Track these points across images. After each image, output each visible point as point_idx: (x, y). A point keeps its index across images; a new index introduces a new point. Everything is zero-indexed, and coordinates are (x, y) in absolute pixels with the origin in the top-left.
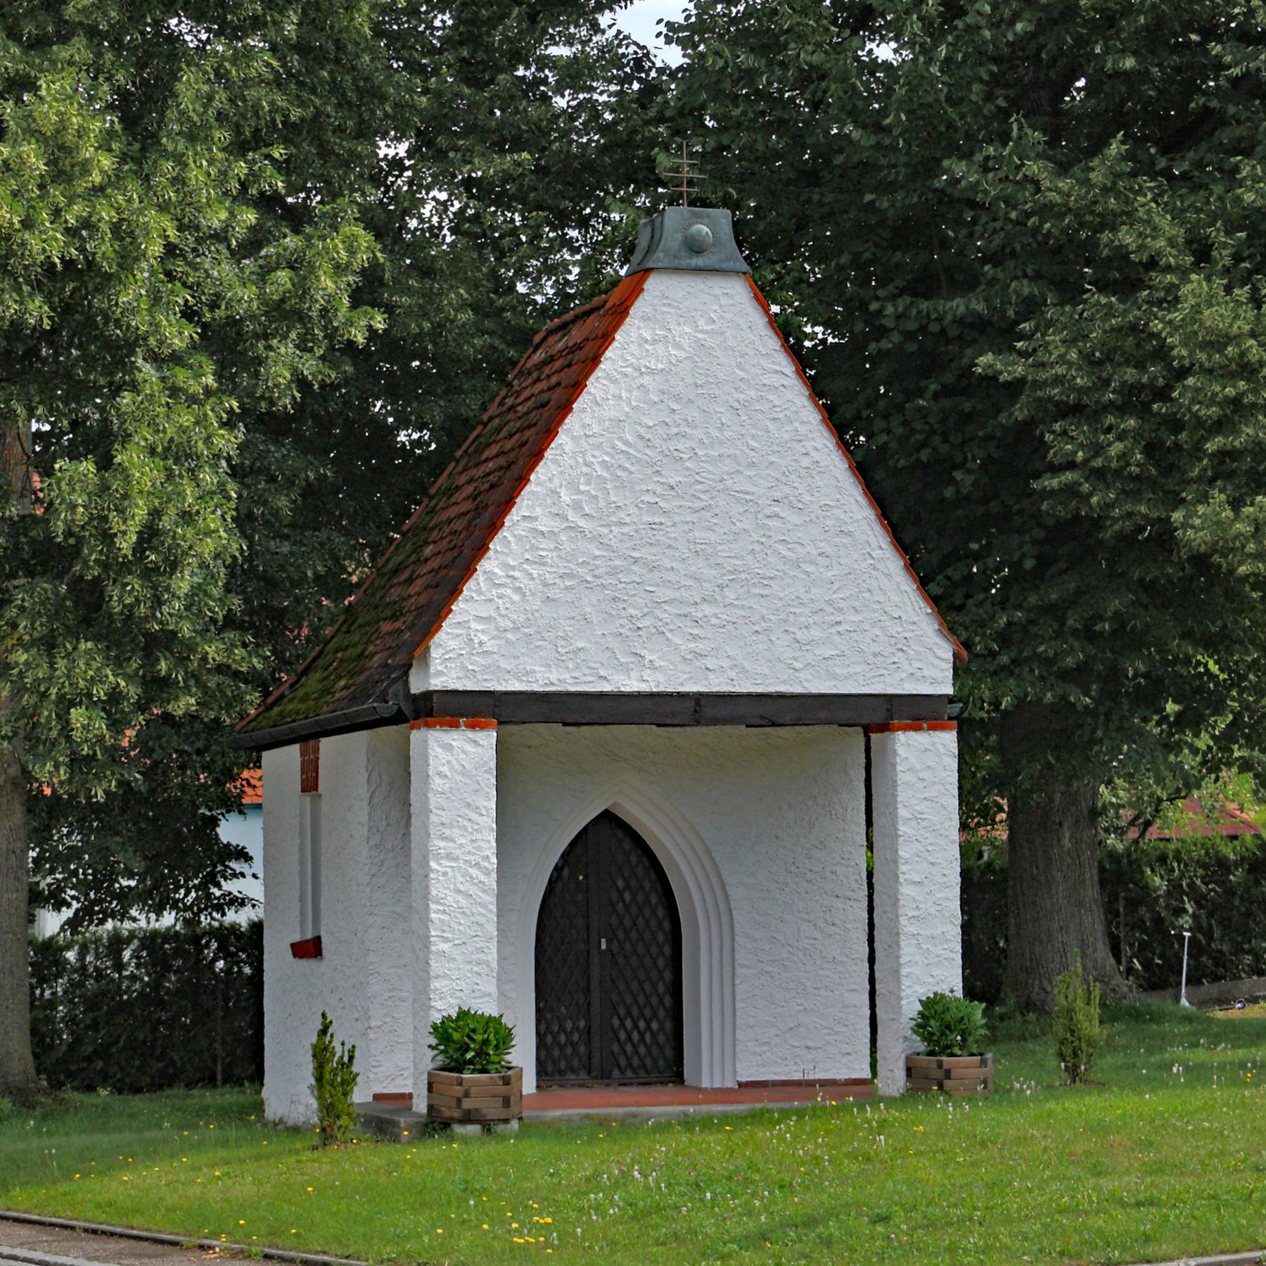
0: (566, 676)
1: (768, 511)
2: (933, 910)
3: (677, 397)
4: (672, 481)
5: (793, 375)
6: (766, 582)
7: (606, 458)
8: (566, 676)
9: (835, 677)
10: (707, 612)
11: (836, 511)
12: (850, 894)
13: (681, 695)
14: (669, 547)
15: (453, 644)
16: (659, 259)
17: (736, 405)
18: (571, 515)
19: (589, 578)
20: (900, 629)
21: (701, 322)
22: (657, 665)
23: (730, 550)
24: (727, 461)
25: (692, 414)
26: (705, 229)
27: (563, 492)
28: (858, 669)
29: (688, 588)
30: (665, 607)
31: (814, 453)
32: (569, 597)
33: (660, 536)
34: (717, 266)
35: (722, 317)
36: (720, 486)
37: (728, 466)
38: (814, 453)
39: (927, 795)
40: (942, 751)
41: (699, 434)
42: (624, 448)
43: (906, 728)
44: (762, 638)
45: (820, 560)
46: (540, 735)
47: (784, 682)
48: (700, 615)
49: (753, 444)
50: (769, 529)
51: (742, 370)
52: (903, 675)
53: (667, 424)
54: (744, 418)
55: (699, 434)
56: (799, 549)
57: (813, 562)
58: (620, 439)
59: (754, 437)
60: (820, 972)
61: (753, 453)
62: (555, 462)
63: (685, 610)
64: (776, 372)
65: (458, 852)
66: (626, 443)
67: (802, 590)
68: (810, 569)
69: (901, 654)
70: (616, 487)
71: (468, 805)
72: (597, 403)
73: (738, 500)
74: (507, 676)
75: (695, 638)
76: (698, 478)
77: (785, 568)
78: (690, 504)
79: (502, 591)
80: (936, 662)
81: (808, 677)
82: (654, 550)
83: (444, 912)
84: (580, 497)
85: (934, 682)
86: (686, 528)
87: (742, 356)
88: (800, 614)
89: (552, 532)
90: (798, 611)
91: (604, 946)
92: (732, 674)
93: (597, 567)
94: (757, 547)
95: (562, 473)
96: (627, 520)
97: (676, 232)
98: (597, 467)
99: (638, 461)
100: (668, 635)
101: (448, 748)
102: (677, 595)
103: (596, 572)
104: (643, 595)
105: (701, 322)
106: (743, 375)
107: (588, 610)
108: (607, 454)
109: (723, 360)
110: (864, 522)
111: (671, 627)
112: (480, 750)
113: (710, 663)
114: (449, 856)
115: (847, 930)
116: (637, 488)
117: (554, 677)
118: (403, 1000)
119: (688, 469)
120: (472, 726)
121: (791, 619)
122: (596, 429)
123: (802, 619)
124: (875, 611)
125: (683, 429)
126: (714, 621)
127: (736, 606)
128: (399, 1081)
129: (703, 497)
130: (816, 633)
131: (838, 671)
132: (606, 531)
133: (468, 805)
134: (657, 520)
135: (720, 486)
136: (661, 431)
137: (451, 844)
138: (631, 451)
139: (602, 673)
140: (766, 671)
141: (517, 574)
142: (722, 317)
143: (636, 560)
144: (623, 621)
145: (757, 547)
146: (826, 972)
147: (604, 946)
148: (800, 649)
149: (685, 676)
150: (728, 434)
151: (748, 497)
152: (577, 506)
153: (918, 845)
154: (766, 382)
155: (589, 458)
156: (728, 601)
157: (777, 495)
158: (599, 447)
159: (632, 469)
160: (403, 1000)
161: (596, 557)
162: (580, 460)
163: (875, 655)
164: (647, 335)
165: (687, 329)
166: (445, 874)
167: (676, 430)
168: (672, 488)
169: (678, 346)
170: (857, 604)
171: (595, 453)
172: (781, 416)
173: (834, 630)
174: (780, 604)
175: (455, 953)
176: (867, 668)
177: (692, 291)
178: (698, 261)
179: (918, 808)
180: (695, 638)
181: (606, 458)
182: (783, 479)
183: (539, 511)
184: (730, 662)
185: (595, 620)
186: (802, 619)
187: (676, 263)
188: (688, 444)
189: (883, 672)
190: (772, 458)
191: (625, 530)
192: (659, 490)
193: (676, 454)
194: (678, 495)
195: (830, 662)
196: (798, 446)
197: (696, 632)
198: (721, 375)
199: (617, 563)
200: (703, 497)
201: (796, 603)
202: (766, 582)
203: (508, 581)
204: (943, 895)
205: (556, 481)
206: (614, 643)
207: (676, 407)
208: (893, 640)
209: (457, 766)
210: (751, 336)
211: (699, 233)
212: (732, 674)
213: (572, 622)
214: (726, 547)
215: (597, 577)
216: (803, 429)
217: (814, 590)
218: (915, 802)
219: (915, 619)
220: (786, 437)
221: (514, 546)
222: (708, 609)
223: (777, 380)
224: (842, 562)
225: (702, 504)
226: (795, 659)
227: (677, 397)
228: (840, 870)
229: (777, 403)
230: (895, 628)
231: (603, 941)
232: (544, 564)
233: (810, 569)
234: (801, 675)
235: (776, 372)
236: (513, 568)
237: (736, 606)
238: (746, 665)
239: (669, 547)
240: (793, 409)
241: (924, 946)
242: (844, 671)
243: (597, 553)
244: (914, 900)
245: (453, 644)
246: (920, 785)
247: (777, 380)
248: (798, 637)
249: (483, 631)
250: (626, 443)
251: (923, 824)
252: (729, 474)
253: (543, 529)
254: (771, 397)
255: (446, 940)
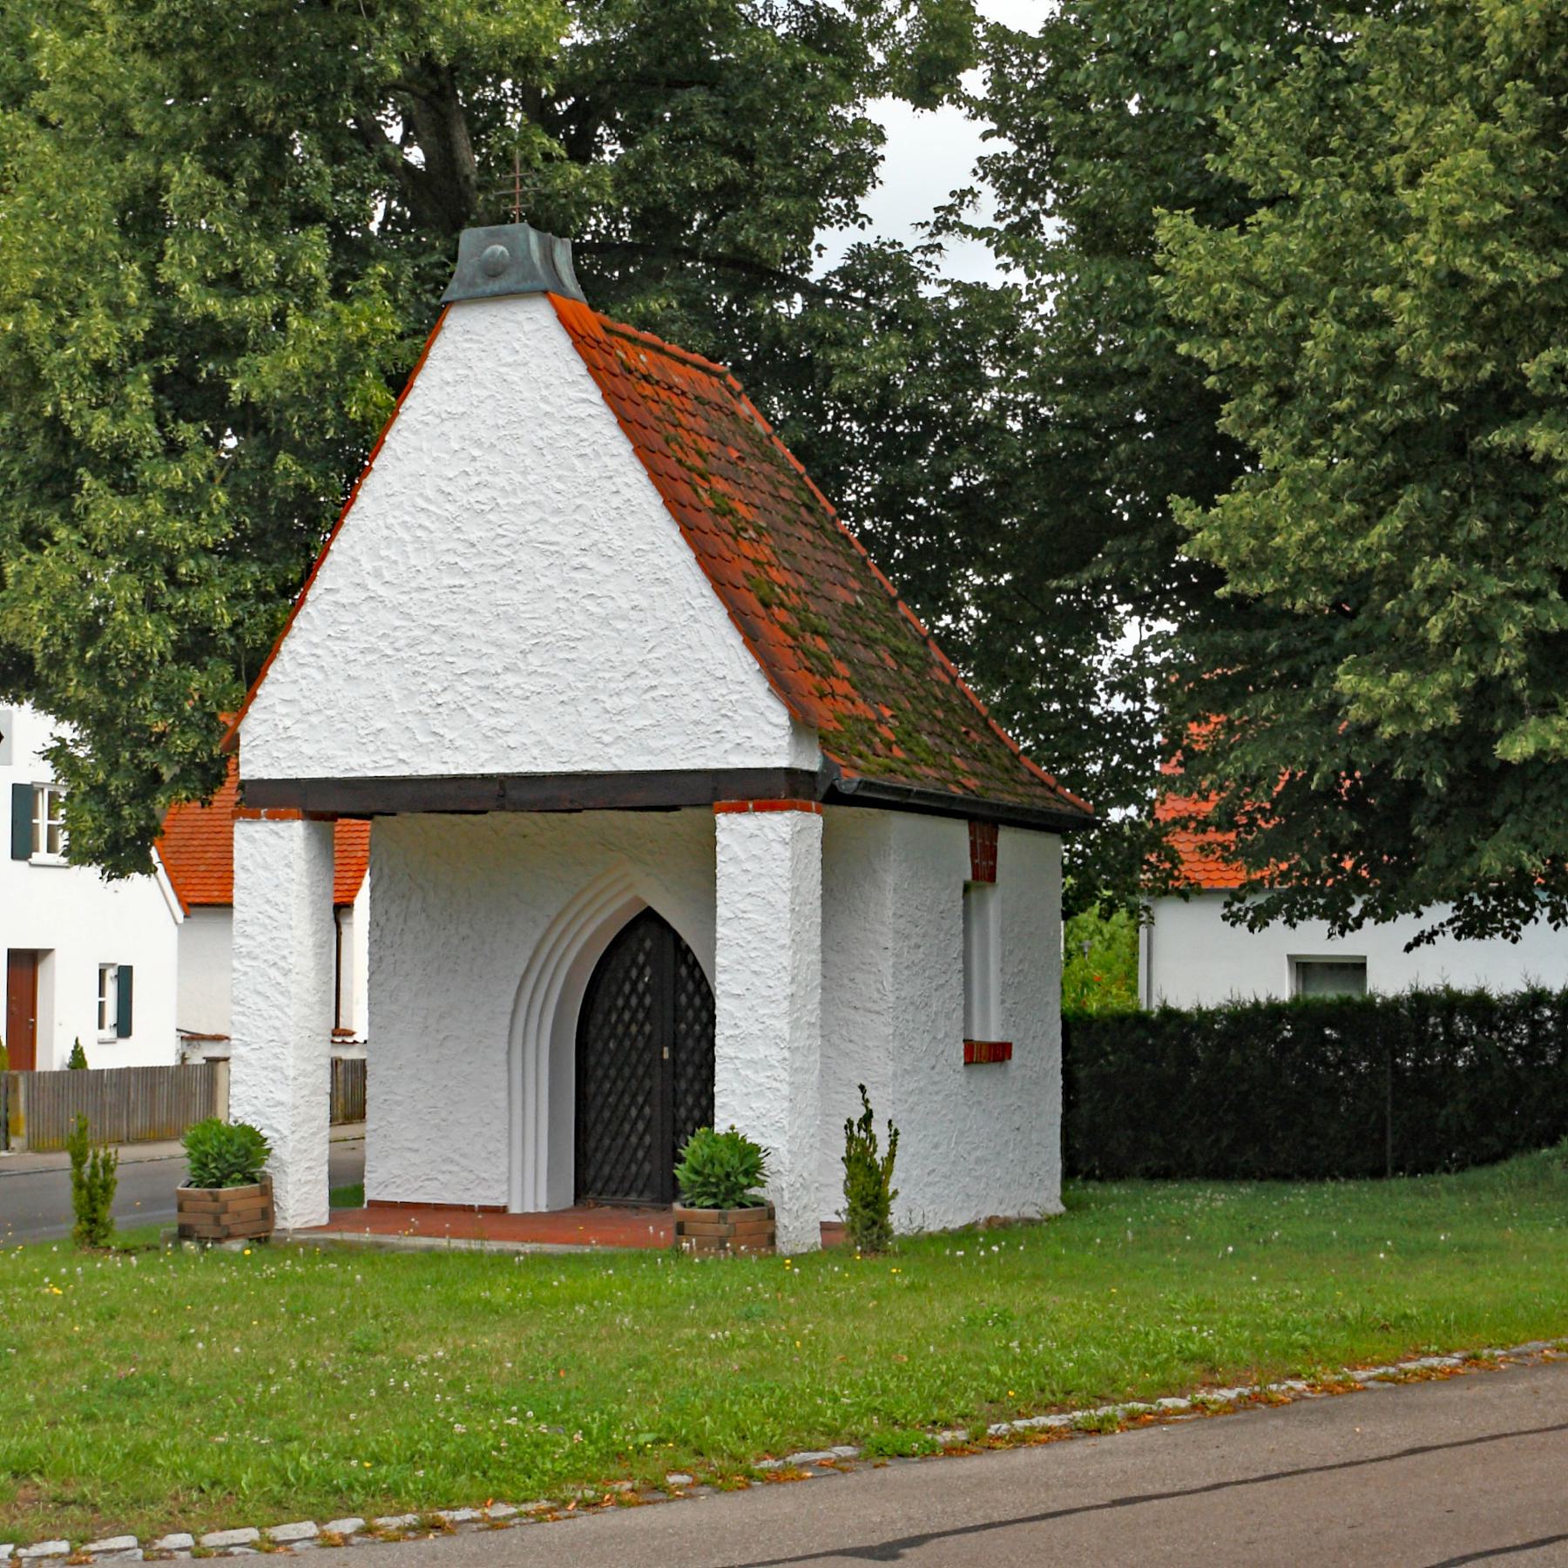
0: (367, 760)
1: (575, 563)
2: (755, 1029)
3: (478, 443)
4: (473, 538)
5: (601, 402)
6: (572, 644)
7: (407, 518)
8: (367, 760)
9: (651, 752)
10: (509, 683)
11: (651, 556)
12: (869, 1005)
13: (485, 778)
14: (470, 611)
15: (260, 730)
16: (453, 290)
17: (540, 444)
18: (372, 583)
19: (389, 652)
20: (724, 691)
21: (504, 353)
22: (457, 744)
23: (534, 611)
24: (531, 509)
25: (496, 460)
26: (501, 248)
27: (364, 559)
28: (674, 741)
29: (490, 656)
30: (466, 679)
31: (624, 490)
32: (371, 674)
33: (459, 599)
34: (514, 288)
35: (526, 346)
36: (523, 538)
37: (533, 514)
38: (624, 490)
39: (751, 890)
40: (771, 836)
41: (500, 481)
42: (425, 505)
43: (728, 810)
44: (571, 709)
45: (634, 615)
46: (535, 823)
47: (592, 758)
48: (501, 686)
49: (559, 486)
50: (576, 583)
51: (548, 402)
52: (728, 746)
53: (467, 473)
54: (549, 457)
55: (500, 481)
56: (610, 604)
57: (624, 618)
58: (421, 495)
59: (559, 478)
60: (834, 1096)
61: (559, 497)
62: (357, 527)
63: (486, 681)
64: (584, 401)
65: (257, 951)
66: (428, 500)
67: (613, 651)
68: (621, 625)
69: (725, 721)
70: (417, 550)
71: (268, 901)
72: (398, 459)
73: (543, 552)
74: (309, 763)
75: (497, 712)
76: (500, 531)
77: (593, 626)
78: (492, 562)
79: (306, 671)
80: (768, 728)
81: (621, 752)
82: (455, 616)
83: (244, 1014)
84: (381, 563)
85: (765, 753)
86: (488, 588)
87: (547, 387)
88: (610, 680)
89: (352, 604)
90: (607, 675)
91: (666, 1056)
92: (536, 752)
93: (397, 639)
94: (562, 605)
95: (363, 538)
96: (427, 584)
97: (472, 256)
98: (397, 528)
99: (439, 518)
100: (470, 710)
101: (251, 839)
102: (477, 665)
103: (396, 645)
104: (444, 667)
105: (504, 353)
106: (548, 409)
107: (389, 687)
108: (408, 513)
109: (526, 394)
110: (682, 566)
111: (473, 701)
112: (281, 842)
113: (512, 740)
114: (249, 955)
115: (866, 1048)
116: (439, 548)
117: (354, 762)
118: (399, 1103)
119: (489, 522)
120: (272, 817)
121: (601, 685)
122: (397, 487)
123: (612, 685)
124: (696, 671)
125: (485, 477)
126: (518, 692)
127: (541, 674)
128: (392, 1189)
129: (505, 552)
130: (628, 700)
131: (653, 744)
132: (405, 598)
133: (268, 901)
134: (457, 582)
135: (523, 538)
136: (462, 482)
137: (251, 942)
138: (432, 508)
139: (402, 755)
140: (573, 747)
141: (319, 652)
142: (526, 346)
143: (436, 629)
144: (424, 698)
145: (562, 605)
146: (841, 1097)
147: (666, 1056)
148: (611, 720)
149: (487, 756)
150: (531, 478)
151: (553, 548)
152: (377, 574)
153: (740, 951)
154: (572, 414)
155: (390, 520)
156: (531, 668)
157: (585, 543)
158: (400, 506)
159: (432, 527)
160: (399, 1103)
161: (396, 628)
162: (381, 523)
163: (697, 723)
164: (448, 376)
165: (489, 364)
166: (245, 974)
167: (476, 480)
168: (473, 545)
169: (480, 384)
170: (675, 664)
171: (397, 513)
172: (588, 451)
173: (647, 696)
174: (587, 668)
175: (252, 1057)
176: (686, 740)
177: (494, 320)
178: (494, 286)
179: (741, 906)
180: (497, 712)
181: (407, 518)
182: (591, 523)
183: (341, 582)
184: (534, 738)
185: (395, 696)
186: (612, 685)
187: (471, 292)
188: (490, 493)
189: (704, 743)
190: (578, 501)
191: (426, 595)
192: (461, 548)
193: (477, 506)
194: (479, 553)
195: (643, 734)
196: (608, 485)
197: (497, 705)
198: (524, 413)
199: (417, 633)
200: (505, 552)
201: (607, 665)
202: (572, 644)
203: (312, 659)
204: (767, 1011)
205: (358, 548)
206: (413, 722)
207: (476, 453)
208: (716, 706)
209: (259, 860)
210: (557, 363)
211: (493, 254)
212: (536, 752)
213: (371, 701)
214: (529, 607)
215: (397, 650)
216: (613, 464)
217: (626, 650)
218: (736, 898)
219: (743, 678)
220: (595, 474)
221: (317, 622)
222: (511, 679)
223: (582, 410)
224: (658, 614)
225: (502, 561)
226: (605, 732)
227: (478, 443)
228: (859, 976)
229: (583, 435)
230: (718, 691)
231: (666, 1049)
232: (346, 639)
233: (621, 625)
234: (611, 751)
235: (584, 401)
236: (316, 645)
237: (541, 674)
238: (551, 740)
239: (470, 611)
240: (602, 441)
241: (743, 1072)
242: (660, 744)
243: (397, 623)
244: (732, 1016)
245: (260, 730)
246: (744, 878)
247: (582, 410)
248: (608, 706)
249: (287, 715)
250: (428, 500)
251: (747, 924)
252: (533, 523)
253: (345, 601)
254: (578, 431)
255: (246, 1044)
